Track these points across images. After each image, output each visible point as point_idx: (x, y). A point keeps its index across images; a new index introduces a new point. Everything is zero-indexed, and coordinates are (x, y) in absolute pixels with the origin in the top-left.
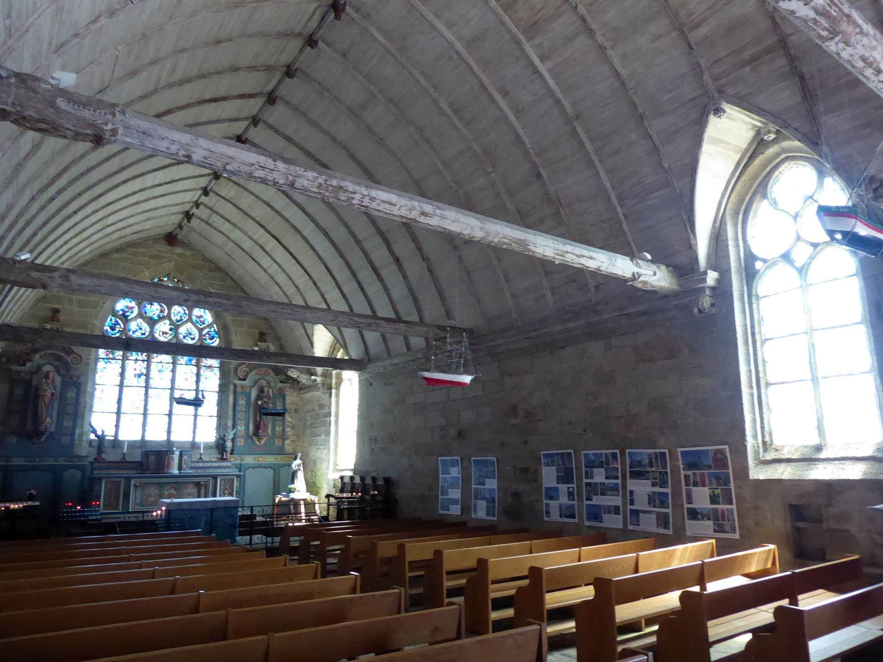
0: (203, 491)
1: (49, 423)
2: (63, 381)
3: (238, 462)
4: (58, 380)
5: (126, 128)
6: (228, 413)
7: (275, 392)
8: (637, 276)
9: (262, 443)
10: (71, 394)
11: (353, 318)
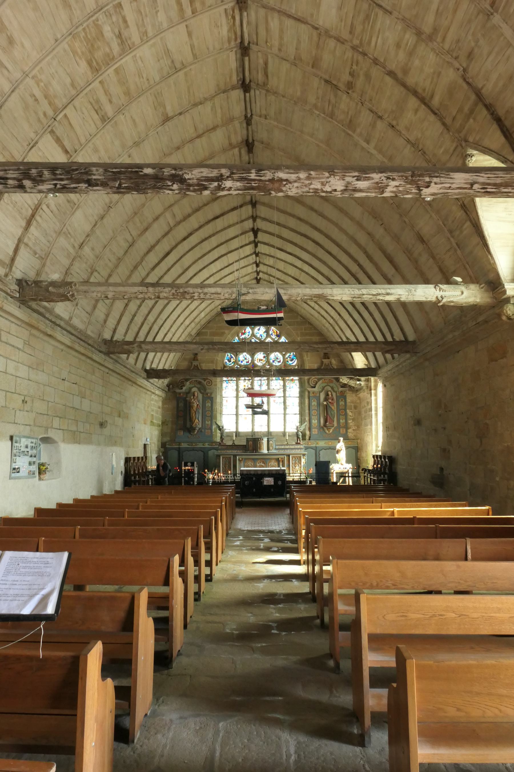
0: (281, 464)
1: (198, 423)
2: (203, 397)
3: (314, 445)
4: (200, 396)
5: (77, 292)
7: (338, 395)
8: (440, 299)
9: (331, 431)
10: (208, 404)
11: (312, 345)
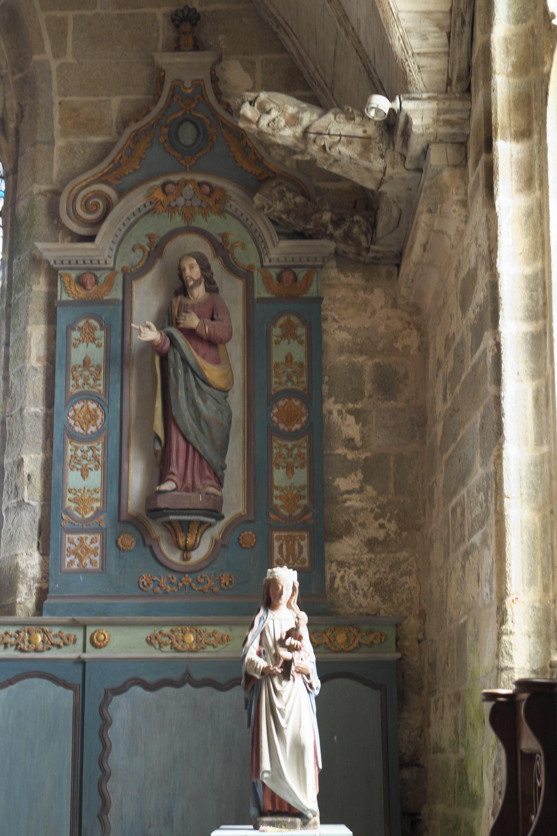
6: (21, 410)
9: (197, 556)
